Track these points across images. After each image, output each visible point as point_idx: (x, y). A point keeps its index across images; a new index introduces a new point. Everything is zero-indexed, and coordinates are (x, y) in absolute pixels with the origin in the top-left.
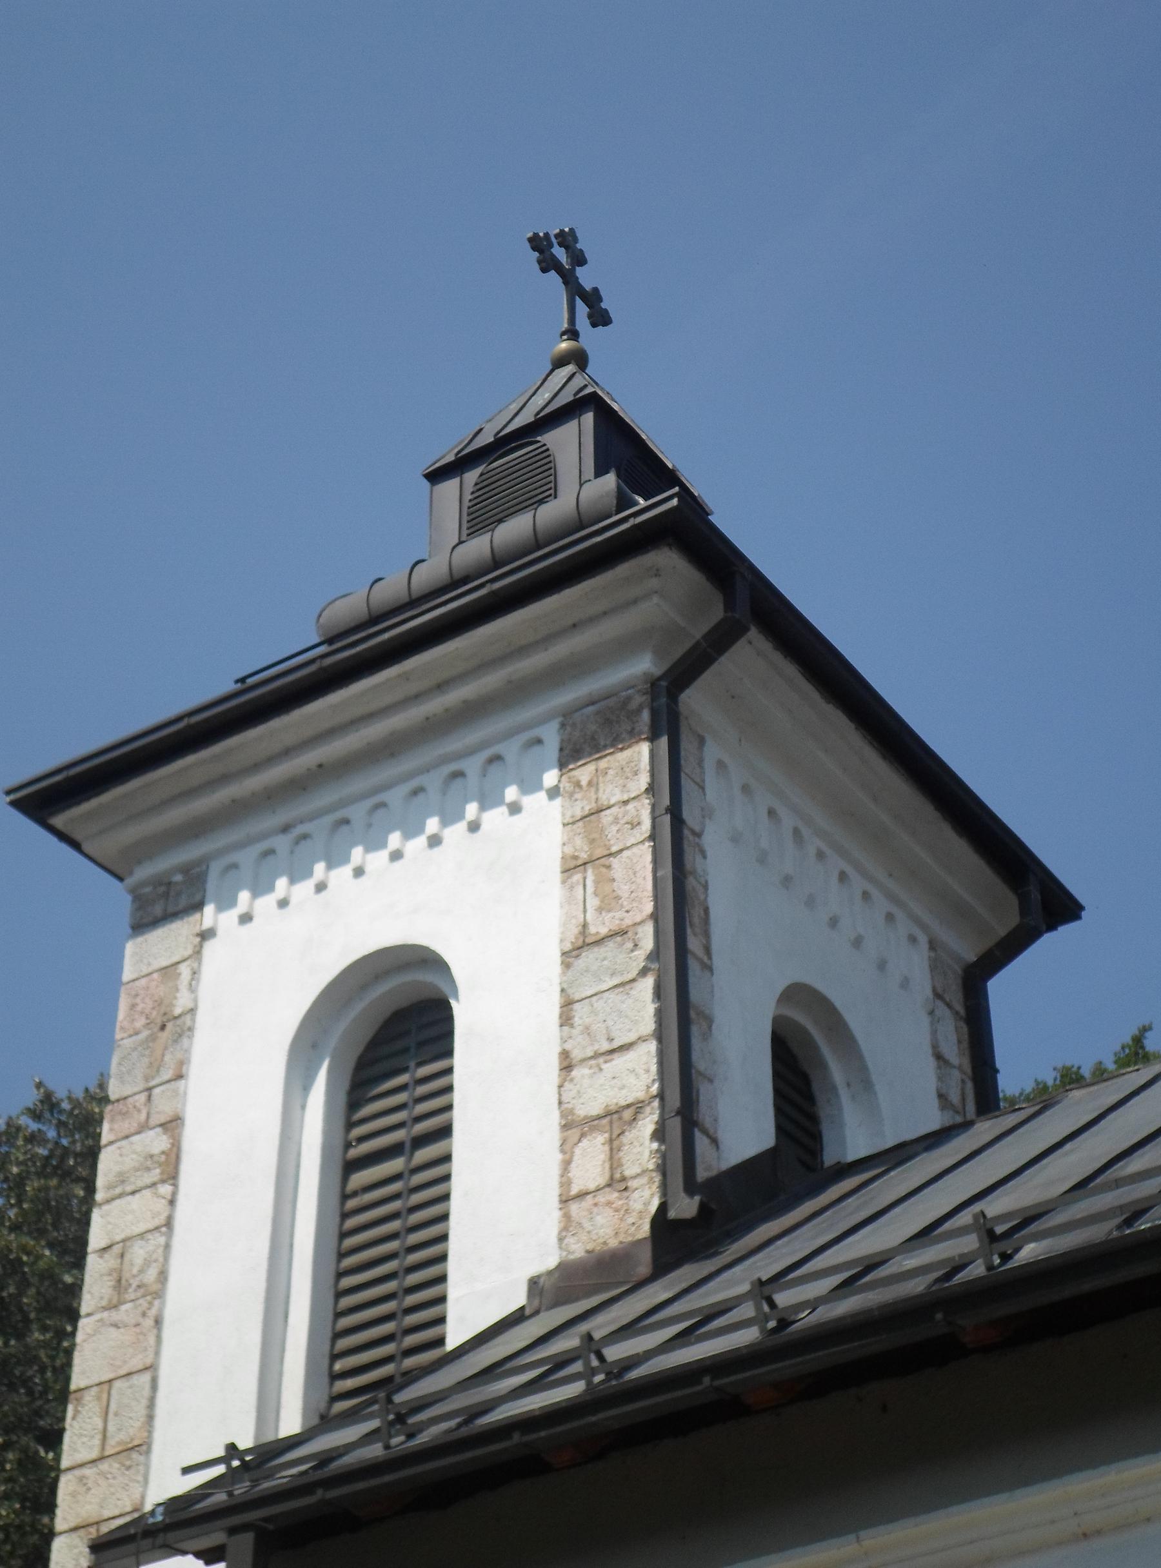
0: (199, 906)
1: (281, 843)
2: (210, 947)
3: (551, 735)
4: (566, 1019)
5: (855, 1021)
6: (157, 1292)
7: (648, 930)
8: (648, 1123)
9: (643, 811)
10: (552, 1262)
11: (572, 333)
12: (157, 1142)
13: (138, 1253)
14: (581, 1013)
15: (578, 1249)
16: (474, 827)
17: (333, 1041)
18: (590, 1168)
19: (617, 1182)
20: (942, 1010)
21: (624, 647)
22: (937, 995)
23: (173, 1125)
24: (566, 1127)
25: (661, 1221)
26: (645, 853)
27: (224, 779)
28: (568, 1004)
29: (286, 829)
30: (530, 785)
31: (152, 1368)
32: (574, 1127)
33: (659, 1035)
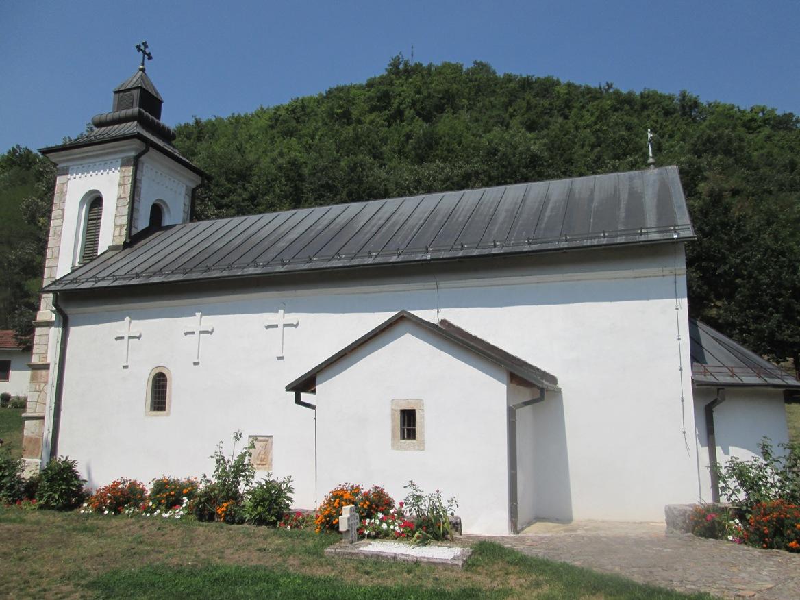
0: (67, 174)
1: (80, 167)
2: (69, 181)
3: (120, 162)
4: (116, 209)
5: (168, 203)
6: (60, 235)
7: (128, 199)
8: (125, 228)
9: (130, 178)
10: (111, 244)
11: (143, 64)
12: (61, 212)
13: (58, 229)
14: (119, 209)
15: (114, 244)
16: (108, 173)
17: (87, 201)
18: (117, 233)
19: (120, 235)
20: (187, 197)
21: (131, 150)
22: (186, 194)
23: (63, 210)
24: (115, 225)
25: (125, 243)
26: (129, 186)
27: (71, 155)
28: (117, 207)
29: (81, 165)
30: (116, 169)
31: (59, 247)
32: (116, 226)
33: (128, 215)
